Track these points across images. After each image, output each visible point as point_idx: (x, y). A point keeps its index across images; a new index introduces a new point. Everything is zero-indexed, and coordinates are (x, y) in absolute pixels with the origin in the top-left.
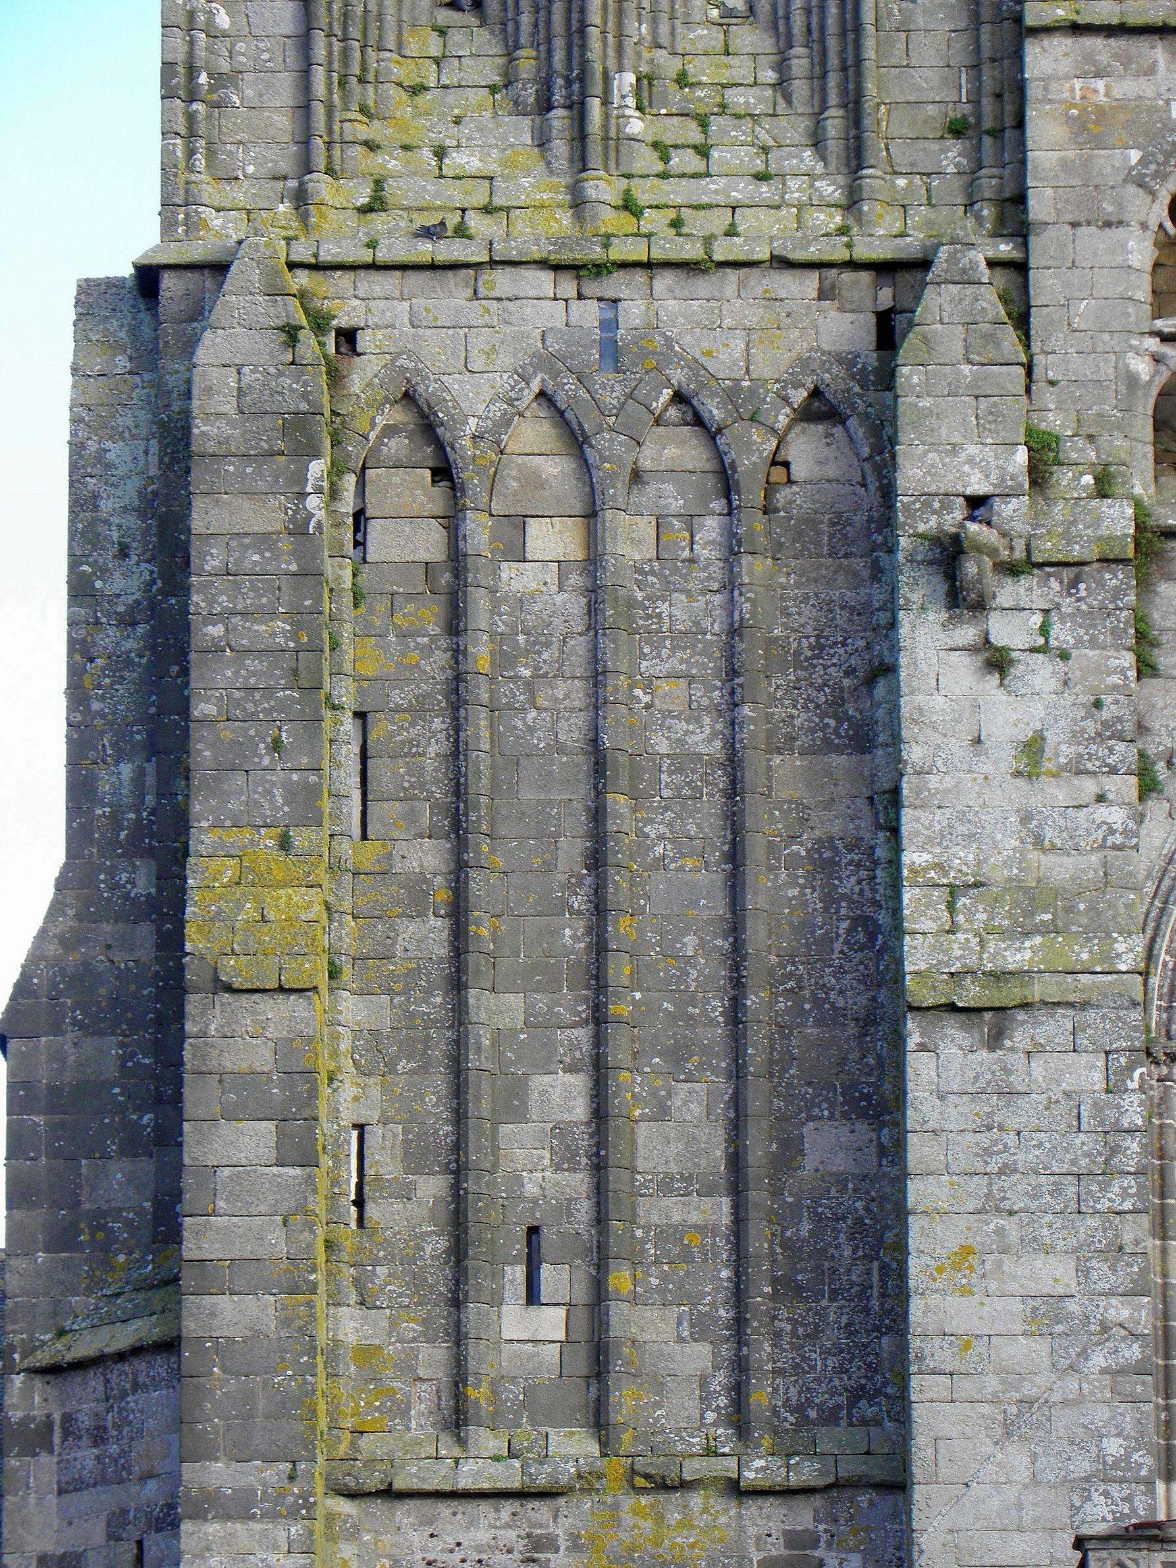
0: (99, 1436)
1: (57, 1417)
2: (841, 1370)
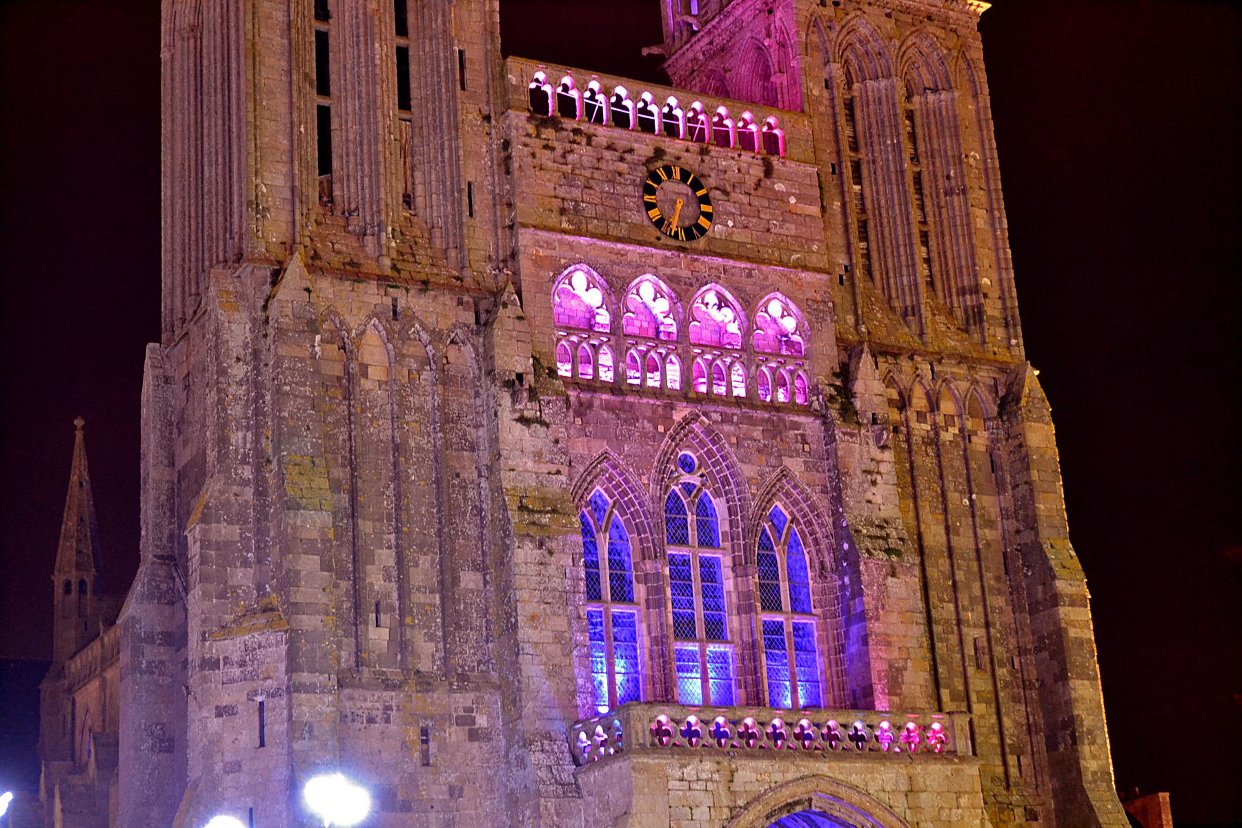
0: (242, 664)
1: (221, 657)
2: (474, 654)
